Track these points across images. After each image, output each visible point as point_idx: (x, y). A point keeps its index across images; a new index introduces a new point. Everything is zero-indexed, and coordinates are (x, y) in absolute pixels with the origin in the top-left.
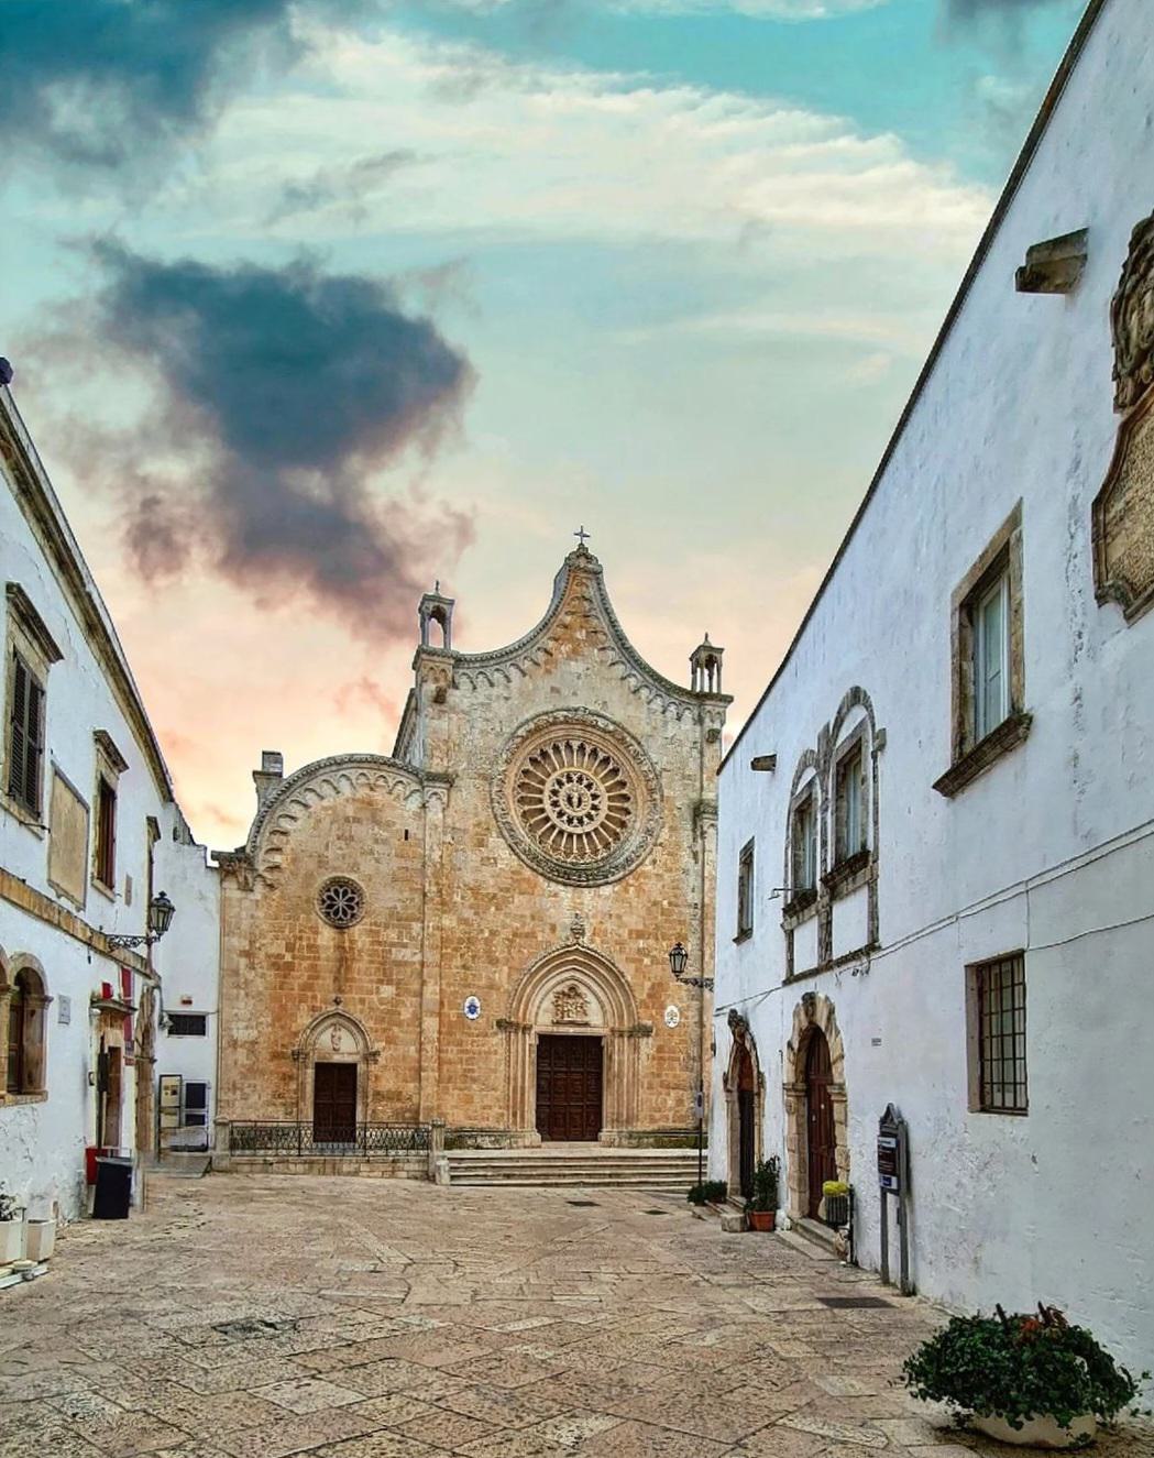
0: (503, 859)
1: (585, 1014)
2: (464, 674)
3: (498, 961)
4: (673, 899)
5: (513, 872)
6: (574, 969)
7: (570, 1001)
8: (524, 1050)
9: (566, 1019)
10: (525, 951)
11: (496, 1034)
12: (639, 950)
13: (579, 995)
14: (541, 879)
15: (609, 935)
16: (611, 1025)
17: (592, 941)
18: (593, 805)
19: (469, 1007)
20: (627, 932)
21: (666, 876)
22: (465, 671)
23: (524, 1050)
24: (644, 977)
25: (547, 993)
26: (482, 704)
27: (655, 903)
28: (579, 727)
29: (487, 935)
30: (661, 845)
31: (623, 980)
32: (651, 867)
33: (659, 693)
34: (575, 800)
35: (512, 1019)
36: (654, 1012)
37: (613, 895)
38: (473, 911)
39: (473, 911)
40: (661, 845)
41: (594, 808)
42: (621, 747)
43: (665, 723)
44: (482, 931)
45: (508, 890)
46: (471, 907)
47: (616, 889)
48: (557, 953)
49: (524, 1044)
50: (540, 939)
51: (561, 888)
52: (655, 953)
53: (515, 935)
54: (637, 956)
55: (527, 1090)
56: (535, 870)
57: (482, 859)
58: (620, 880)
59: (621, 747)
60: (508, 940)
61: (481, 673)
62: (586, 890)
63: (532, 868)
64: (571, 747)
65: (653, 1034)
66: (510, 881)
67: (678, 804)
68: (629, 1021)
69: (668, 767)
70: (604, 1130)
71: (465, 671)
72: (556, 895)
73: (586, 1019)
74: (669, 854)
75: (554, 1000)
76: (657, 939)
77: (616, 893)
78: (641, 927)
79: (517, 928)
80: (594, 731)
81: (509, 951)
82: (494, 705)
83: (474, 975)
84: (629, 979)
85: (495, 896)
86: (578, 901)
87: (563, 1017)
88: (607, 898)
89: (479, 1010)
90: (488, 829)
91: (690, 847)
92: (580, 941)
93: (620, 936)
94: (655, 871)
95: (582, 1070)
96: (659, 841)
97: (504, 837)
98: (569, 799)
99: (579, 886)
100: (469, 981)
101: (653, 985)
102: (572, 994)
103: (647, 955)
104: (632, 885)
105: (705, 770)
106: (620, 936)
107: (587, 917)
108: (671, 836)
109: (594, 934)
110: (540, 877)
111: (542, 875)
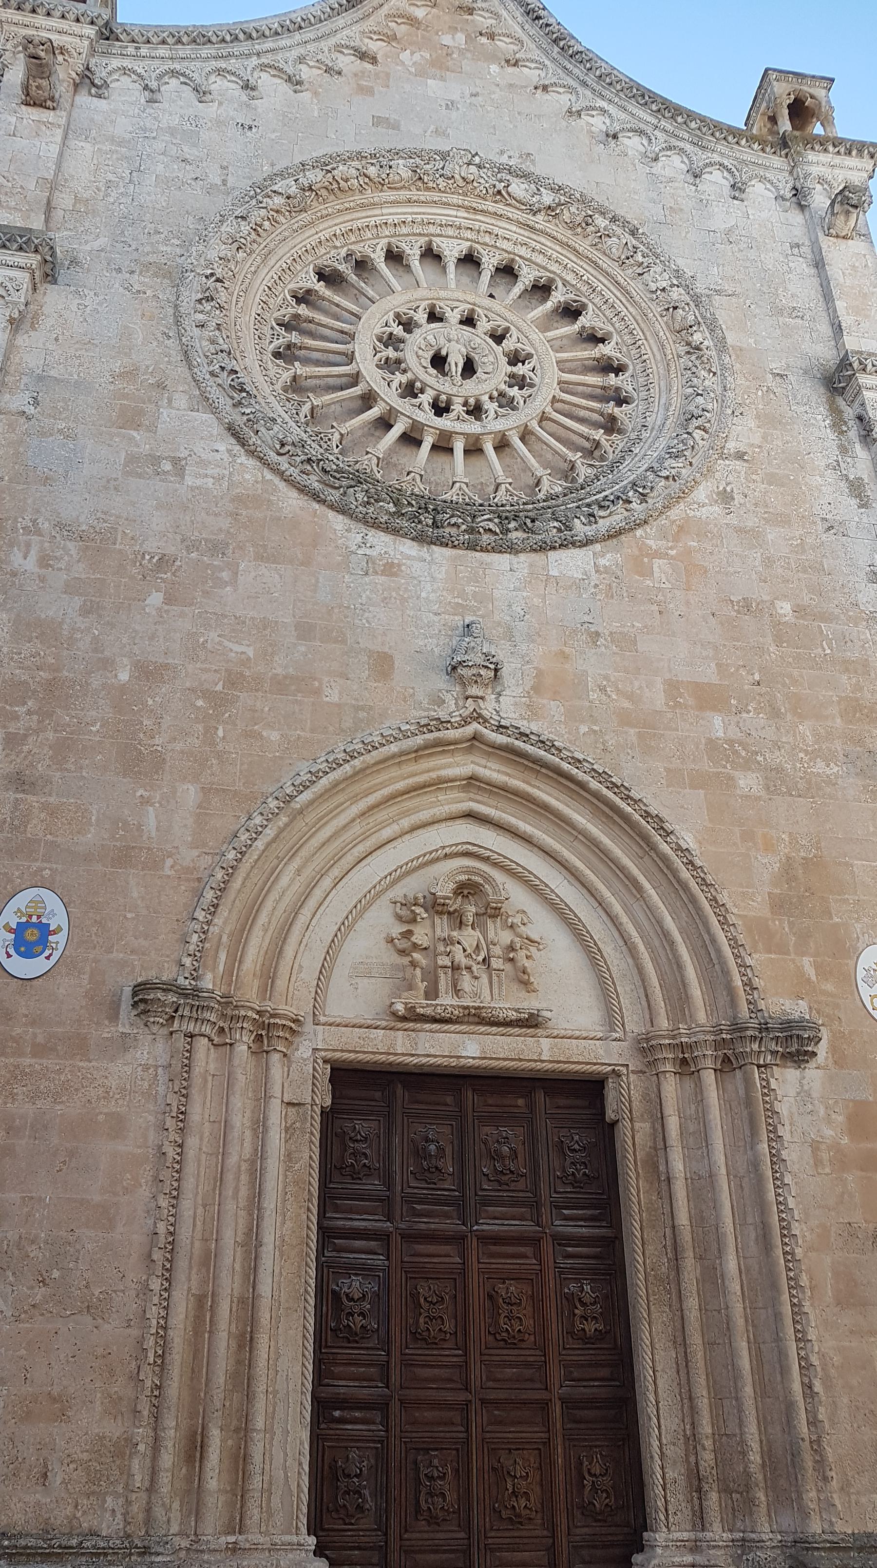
0: (203, 463)
1: (524, 981)
2: (125, 71)
3: (158, 762)
4: (806, 598)
5: (238, 499)
6: (470, 815)
7: (469, 937)
8: (260, 1126)
9: (447, 1001)
10: (275, 736)
11: (125, 1043)
12: (712, 744)
13: (493, 912)
14: (338, 522)
15: (593, 696)
16: (634, 1024)
17: (533, 712)
18: (512, 376)
19: (19, 931)
20: (660, 686)
21: (772, 534)
22: (127, 63)
23: (260, 1126)
24: (748, 836)
25: (361, 908)
26: (172, 131)
27: (746, 606)
28: (455, 199)
29: (124, 676)
30: (740, 456)
31: (665, 848)
32: (717, 509)
33: (674, 142)
34: (456, 362)
35: (207, 982)
36: (807, 964)
37: (594, 577)
38: (78, 601)
39: (78, 601)
40: (740, 456)
41: (515, 359)
42: (583, 245)
43: (703, 204)
44: (107, 664)
45: (216, 548)
46: (70, 589)
47: (602, 562)
48: (394, 748)
49: (262, 1097)
50: (332, 695)
51: (409, 548)
52: (777, 758)
53: (234, 680)
54: (706, 766)
55: (264, 1317)
56: (315, 497)
57: (132, 459)
58: (615, 534)
59: (583, 245)
60: (207, 694)
61: (174, 73)
62: (502, 561)
63: (303, 490)
64: (438, 258)
65: (822, 1049)
66: (225, 523)
67: (776, 366)
68: (712, 1007)
69: (729, 288)
70: (660, 1537)
71: (127, 63)
72: (390, 569)
73: (530, 1003)
74: (771, 479)
75: (397, 929)
76: (775, 714)
77: (607, 569)
78: (709, 674)
79: (246, 662)
80: (500, 208)
81: (209, 732)
82: (204, 135)
83: (53, 812)
84: (689, 840)
85: (164, 562)
86: (469, 589)
87: (432, 993)
88: (577, 585)
89: (59, 940)
90: (161, 386)
91: (837, 467)
92: (488, 708)
93: (630, 697)
94: (733, 520)
95: (528, 1227)
96: (731, 446)
97: (214, 410)
98: (439, 361)
99: (472, 546)
100: (35, 828)
101: (788, 865)
102: (471, 910)
103: (747, 765)
104: (657, 554)
105: (836, 293)
106: (630, 697)
107: (509, 635)
108: (764, 437)
109: (537, 689)
110: (331, 514)
111: (342, 510)
